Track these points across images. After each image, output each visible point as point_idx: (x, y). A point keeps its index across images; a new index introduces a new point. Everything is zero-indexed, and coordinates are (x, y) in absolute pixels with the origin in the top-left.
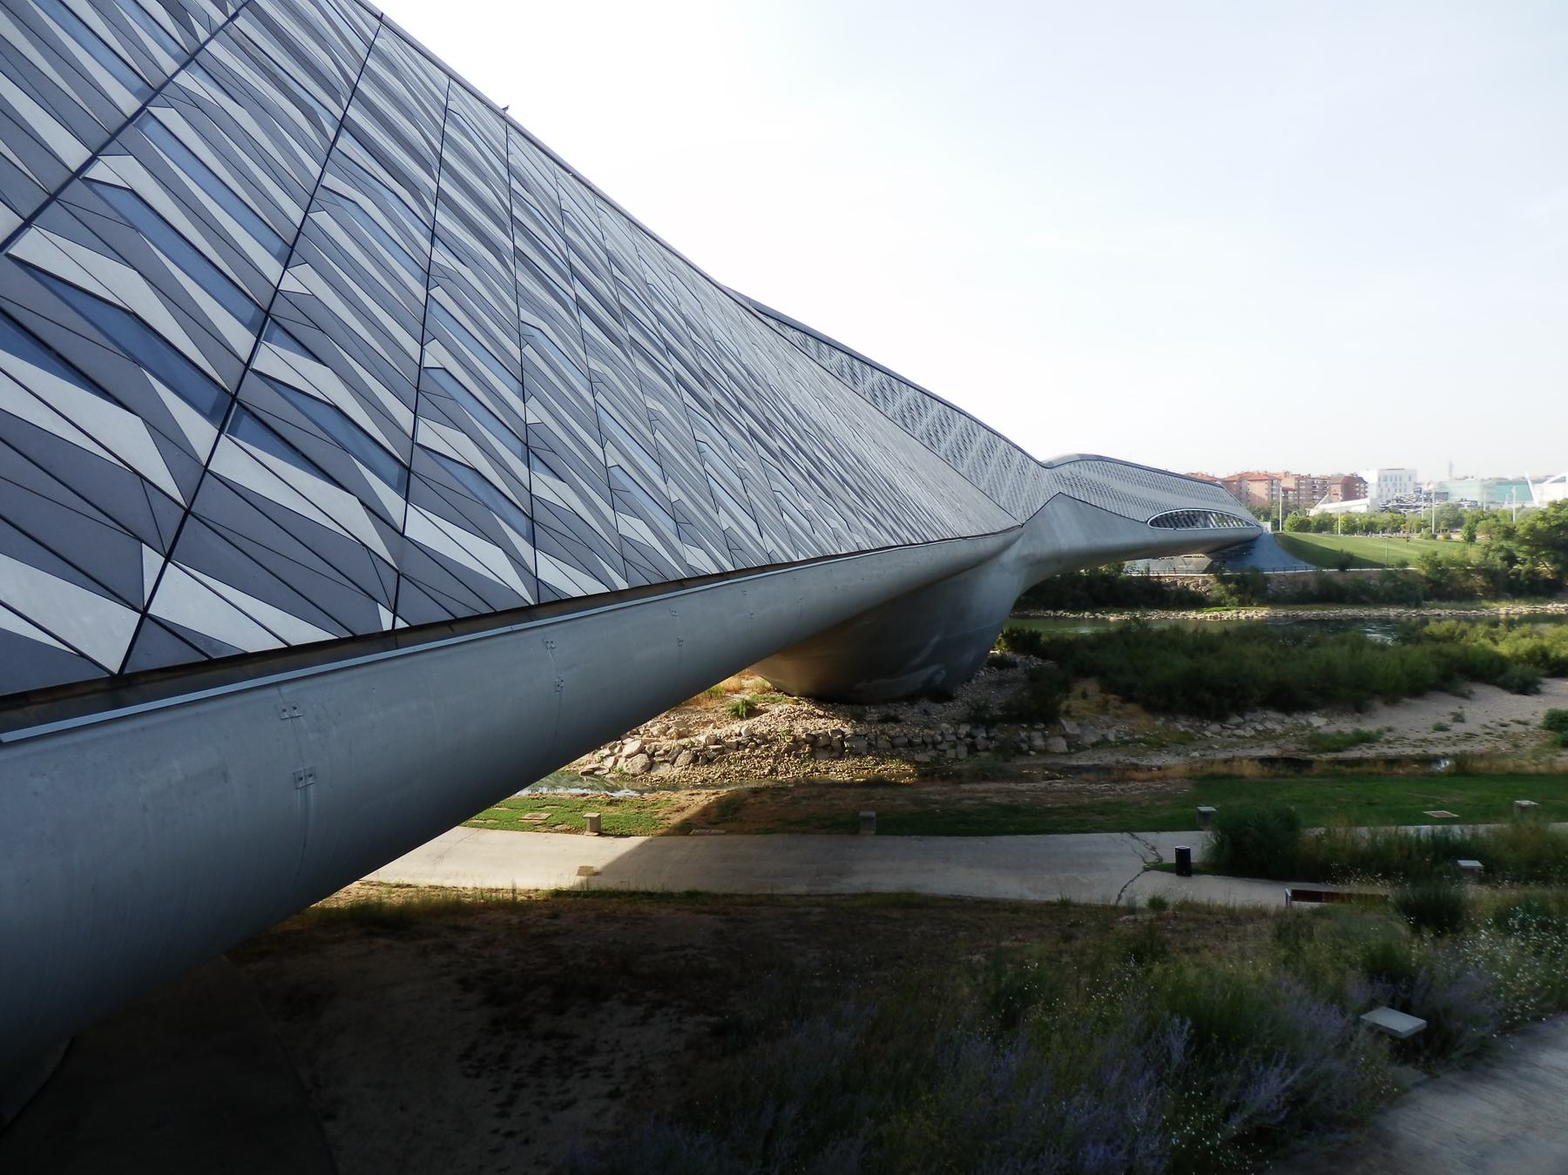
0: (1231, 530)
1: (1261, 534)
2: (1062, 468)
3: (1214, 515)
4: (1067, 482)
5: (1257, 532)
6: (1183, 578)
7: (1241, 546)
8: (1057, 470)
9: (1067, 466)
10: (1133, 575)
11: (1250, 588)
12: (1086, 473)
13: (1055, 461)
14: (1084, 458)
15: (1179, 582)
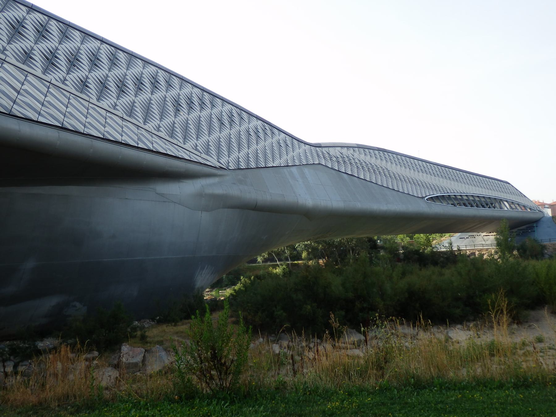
0: (519, 213)
1: (542, 217)
2: (330, 149)
3: (506, 203)
4: (334, 159)
5: (541, 216)
6: (480, 250)
7: (527, 226)
8: (324, 150)
9: (339, 149)
10: (442, 250)
11: (528, 253)
12: (361, 156)
13: (323, 143)
14: (359, 147)
15: (477, 253)
